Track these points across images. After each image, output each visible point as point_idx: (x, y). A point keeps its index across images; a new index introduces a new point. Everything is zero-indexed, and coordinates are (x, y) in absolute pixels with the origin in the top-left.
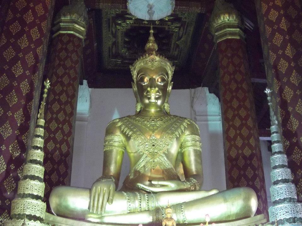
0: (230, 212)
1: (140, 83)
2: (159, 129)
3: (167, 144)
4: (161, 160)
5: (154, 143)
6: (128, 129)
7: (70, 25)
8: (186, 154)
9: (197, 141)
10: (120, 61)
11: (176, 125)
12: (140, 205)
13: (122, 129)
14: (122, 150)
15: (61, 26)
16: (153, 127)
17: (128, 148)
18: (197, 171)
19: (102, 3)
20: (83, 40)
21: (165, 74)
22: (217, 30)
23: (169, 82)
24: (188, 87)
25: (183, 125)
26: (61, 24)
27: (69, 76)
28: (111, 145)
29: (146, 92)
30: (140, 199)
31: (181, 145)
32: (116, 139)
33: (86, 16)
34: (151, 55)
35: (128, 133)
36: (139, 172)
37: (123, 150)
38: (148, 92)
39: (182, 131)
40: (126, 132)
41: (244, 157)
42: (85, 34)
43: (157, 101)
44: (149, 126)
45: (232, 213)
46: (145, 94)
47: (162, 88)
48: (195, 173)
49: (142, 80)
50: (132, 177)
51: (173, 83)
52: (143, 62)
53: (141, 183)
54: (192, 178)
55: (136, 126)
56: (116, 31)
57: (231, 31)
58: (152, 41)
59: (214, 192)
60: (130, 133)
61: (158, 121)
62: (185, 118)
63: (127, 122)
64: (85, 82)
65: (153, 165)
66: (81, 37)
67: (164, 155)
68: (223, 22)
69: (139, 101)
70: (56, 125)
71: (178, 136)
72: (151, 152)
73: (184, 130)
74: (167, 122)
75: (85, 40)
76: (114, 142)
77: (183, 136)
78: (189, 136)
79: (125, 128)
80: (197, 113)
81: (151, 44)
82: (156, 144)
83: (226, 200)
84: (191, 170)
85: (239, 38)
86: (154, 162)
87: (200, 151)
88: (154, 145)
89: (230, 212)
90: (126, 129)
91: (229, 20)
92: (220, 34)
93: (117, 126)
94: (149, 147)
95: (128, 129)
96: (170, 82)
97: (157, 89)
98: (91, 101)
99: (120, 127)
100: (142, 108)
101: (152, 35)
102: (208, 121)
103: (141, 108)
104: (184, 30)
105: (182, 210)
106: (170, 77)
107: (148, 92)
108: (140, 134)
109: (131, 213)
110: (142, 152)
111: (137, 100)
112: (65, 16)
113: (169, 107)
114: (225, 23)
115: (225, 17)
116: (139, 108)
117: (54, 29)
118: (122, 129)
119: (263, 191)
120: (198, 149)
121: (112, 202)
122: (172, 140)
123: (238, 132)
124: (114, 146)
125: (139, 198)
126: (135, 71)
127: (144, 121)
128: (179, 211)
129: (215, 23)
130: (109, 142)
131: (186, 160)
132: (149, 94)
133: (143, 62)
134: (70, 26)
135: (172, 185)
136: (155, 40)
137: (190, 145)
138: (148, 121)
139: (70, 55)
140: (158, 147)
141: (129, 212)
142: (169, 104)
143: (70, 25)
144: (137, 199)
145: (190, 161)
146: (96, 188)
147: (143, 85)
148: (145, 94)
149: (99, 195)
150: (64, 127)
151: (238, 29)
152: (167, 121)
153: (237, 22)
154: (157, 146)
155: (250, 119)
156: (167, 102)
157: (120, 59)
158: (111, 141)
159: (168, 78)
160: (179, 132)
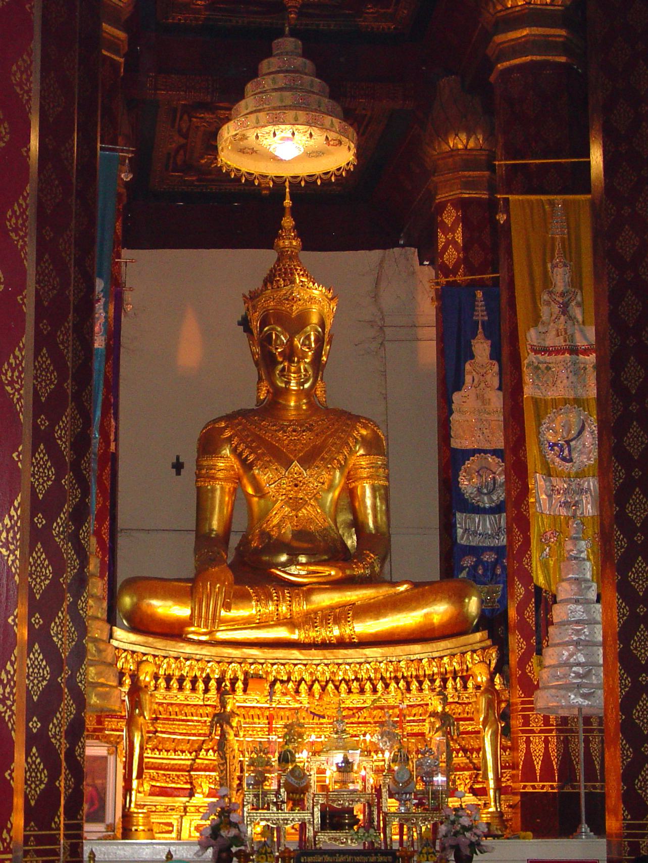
3: (322, 481)
6: (246, 448)
16: (295, 446)
31: (349, 473)
50: (254, 544)
56: (188, 129)
57: (469, 176)
61: (304, 431)
72: (291, 498)
82: (300, 482)
85: (486, 196)
88: (296, 485)
91: (466, 147)
95: (246, 448)
108: (270, 461)
111: (259, 373)
124: (217, 479)
125: (276, 598)
127: (276, 431)
137: (365, 475)
138: (285, 432)
149: (209, 598)
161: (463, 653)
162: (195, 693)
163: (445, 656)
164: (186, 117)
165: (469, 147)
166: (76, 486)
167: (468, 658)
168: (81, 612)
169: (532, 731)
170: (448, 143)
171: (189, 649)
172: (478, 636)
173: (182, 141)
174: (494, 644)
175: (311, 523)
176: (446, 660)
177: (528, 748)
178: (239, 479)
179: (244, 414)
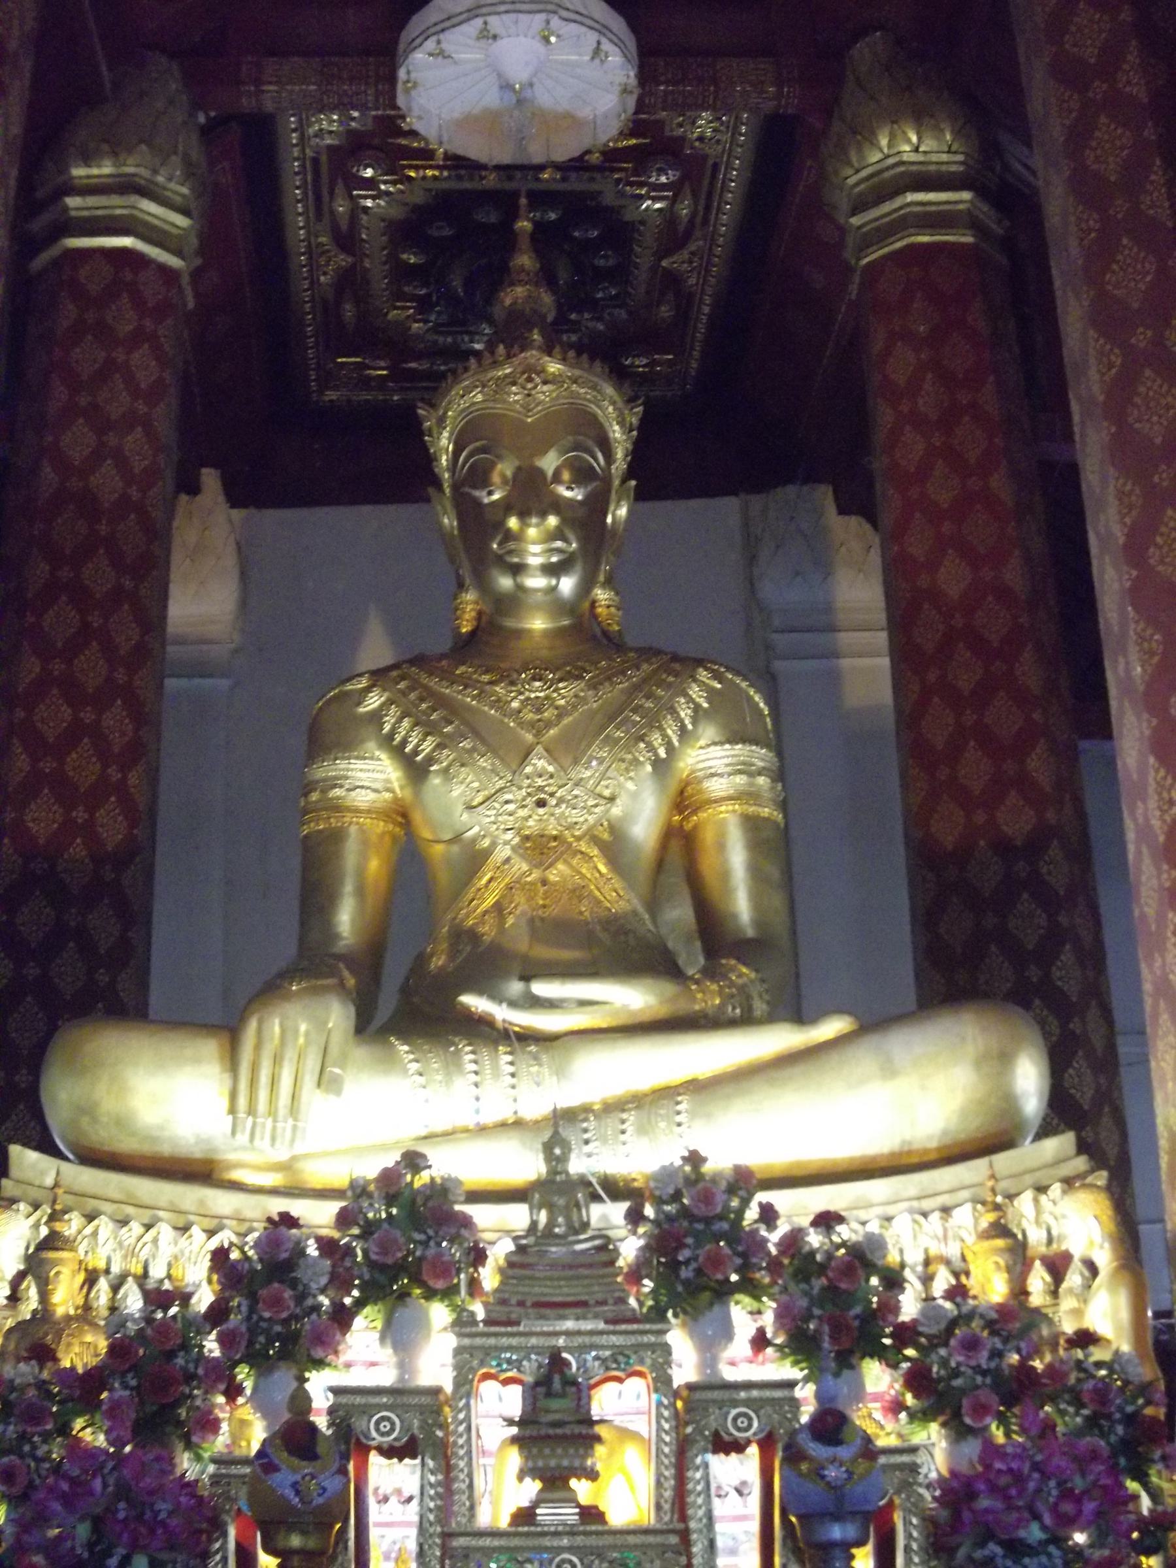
1: (469, 494)
2: (567, 721)
3: (607, 793)
4: (579, 873)
5: (541, 789)
7: (116, 205)
8: (708, 836)
9: (760, 774)
10: (382, 364)
11: (648, 697)
13: (387, 728)
14: (391, 827)
15: (73, 213)
16: (539, 711)
17: (417, 817)
18: (758, 923)
19: (276, 83)
20: (185, 280)
21: (590, 443)
22: (859, 206)
23: (616, 482)
25: (686, 695)
26: (73, 202)
27: (122, 463)
28: (337, 808)
29: (499, 538)
32: (359, 774)
33: (196, 154)
34: (523, 349)
35: (418, 745)
36: (473, 936)
37: (398, 829)
39: (683, 728)
40: (404, 742)
41: (1003, 847)
42: (194, 242)
43: (554, 582)
44: (515, 704)
46: (495, 546)
47: (581, 513)
48: (750, 933)
49: (479, 476)
50: (438, 962)
51: (633, 483)
52: (484, 386)
53: (480, 992)
54: (733, 962)
55: (452, 710)
58: (528, 274)
59: (832, 1027)
60: (428, 746)
61: (561, 680)
62: (700, 662)
64: (210, 479)
65: (541, 902)
66: (174, 261)
67: (595, 852)
68: (891, 161)
69: (468, 581)
70: (67, 712)
71: (662, 753)
74: (607, 684)
75: (197, 275)
76: (349, 790)
77: (689, 751)
78: (716, 751)
79: (400, 720)
80: (777, 622)
81: (520, 291)
82: (552, 795)
84: (735, 916)
85: (969, 239)
86: (544, 882)
87: (775, 823)
88: (541, 804)
90: (406, 723)
93: (361, 710)
94: (522, 813)
96: (624, 481)
97: (552, 521)
98: (244, 576)
99: (376, 717)
100: (484, 619)
101: (524, 243)
102: (836, 655)
103: (480, 614)
104: (696, 203)
105: (678, 1119)
106: (619, 454)
107: (509, 536)
110: (484, 836)
112: (87, 159)
113: (618, 609)
114: (902, 163)
115: (899, 132)
116: (467, 616)
117: (38, 225)
118: (387, 728)
119: (1093, 1013)
120: (766, 812)
122: (632, 774)
123: (969, 718)
124: (349, 809)
125: (474, 1067)
128: (662, 1125)
129: (849, 163)
130: (324, 791)
131: (708, 865)
132: (512, 545)
133: (484, 386)
134: (118, 212)
136: (542, 269)
138: (513, 683)
139: (120, 355)
140: (563, 813)
142: (617, 594)
143: (116, 205)
145: (725, 875)
146: (260, 1023)
147: (486, 501)
148: (495, 546)
149: (277, 1060)
150: (108, 720)
151: (966, 195)
152: (609, 678)
153: (960, 158)
154: (557, 805)
155: (1028, 654)
156: (609, 583)
157: (379, 358)
158: (335, 786)
160: (665, 736)
164: (340, 189)
175: (580, 898)
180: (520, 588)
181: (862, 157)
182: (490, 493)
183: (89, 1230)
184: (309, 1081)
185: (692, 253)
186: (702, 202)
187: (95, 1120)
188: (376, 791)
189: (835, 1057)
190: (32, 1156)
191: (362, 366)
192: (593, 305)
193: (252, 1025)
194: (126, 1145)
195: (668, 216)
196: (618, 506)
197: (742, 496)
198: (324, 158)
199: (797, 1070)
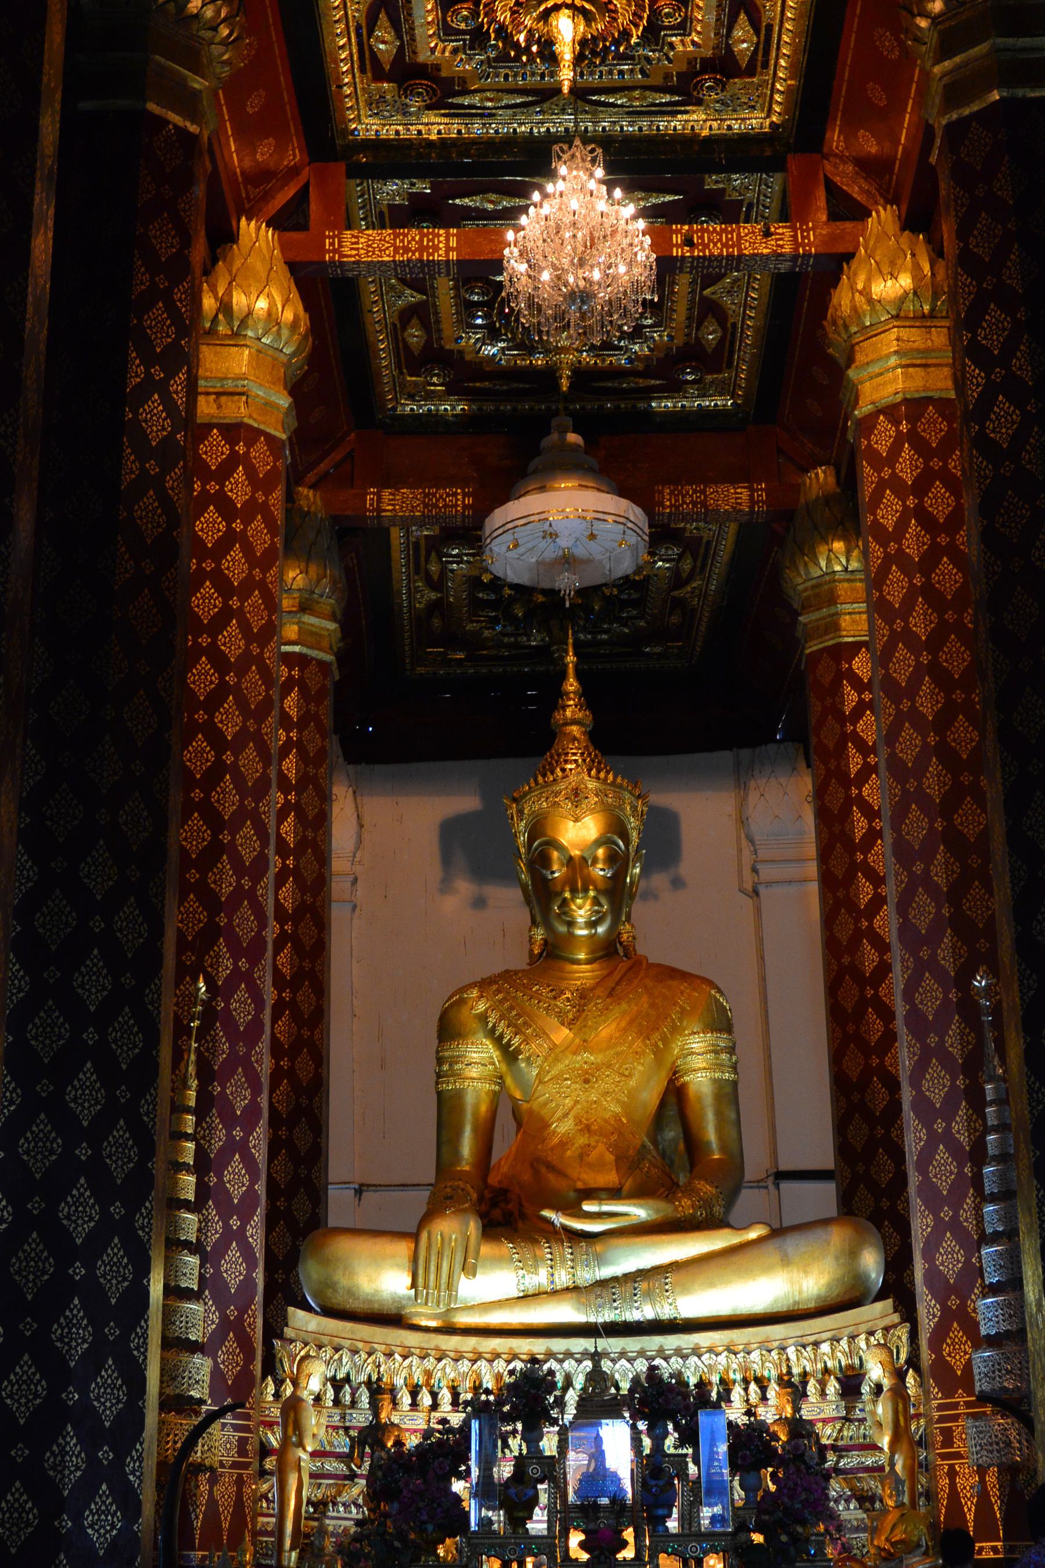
0: (800, 1292)
3: (627, 1073)
12: (552, 1275)
24: (729, 748)
30: (551, 1260)
35: (510, 1040)
38: (565, 903)
40: (501, 1037)
43: (593, 931)
45: (805, 1295)
63: (505, 999)
68: (827, 578)
73: (681, 1020)
83: (786, 1261)
89: (800, 1292)
90: (502, 1024)
92: (817, 620)
99: (483, 1018)
106: (634, 836)
109: (527, 1298)
111: (531, 912)
118: (490, 1025)
121: (474, 1275)
125: (549, 1256)
126: (523, 824)
135: (639, 1212)
137: (701, 1066)
141: (521, 1294)
144: (544, 1260)
149: (440, 1254)
158: (457, 1063)
159: (627, 843)
161: (853, 1338)
162: (417, 1411)
163: (824, 1341)
165: (850, 568)
166: (135, 1029)
167: (863, 1345)
168: (140, 1233)
169: (958, 1456)
170: (818, 565)
171: (412, 1339)
172: (879, 1306)
173: (433, 596)
174: (904, 1320)
176: (825, 1348)
177: (953, 1485)
178: (501, 1078)
179: (507, 976)
180: (571, 934)
181: (808, 572)
182: (553, 873)
183: (336, 1357)
184: (458, 1267)
185: (694, 588)
186: (699, 564)
187: (335, 1291)
188: (485, 1065)
189: (755, 1252)
190: (301, 1313)
191: (444, 654)
192: (619, 620)
193: (424, 1235)
194: (351, 1305)
195: (676, 572)
196: (634, 867)
197: (735, 750)
198: (423, 542)
199: (735, 1258)
